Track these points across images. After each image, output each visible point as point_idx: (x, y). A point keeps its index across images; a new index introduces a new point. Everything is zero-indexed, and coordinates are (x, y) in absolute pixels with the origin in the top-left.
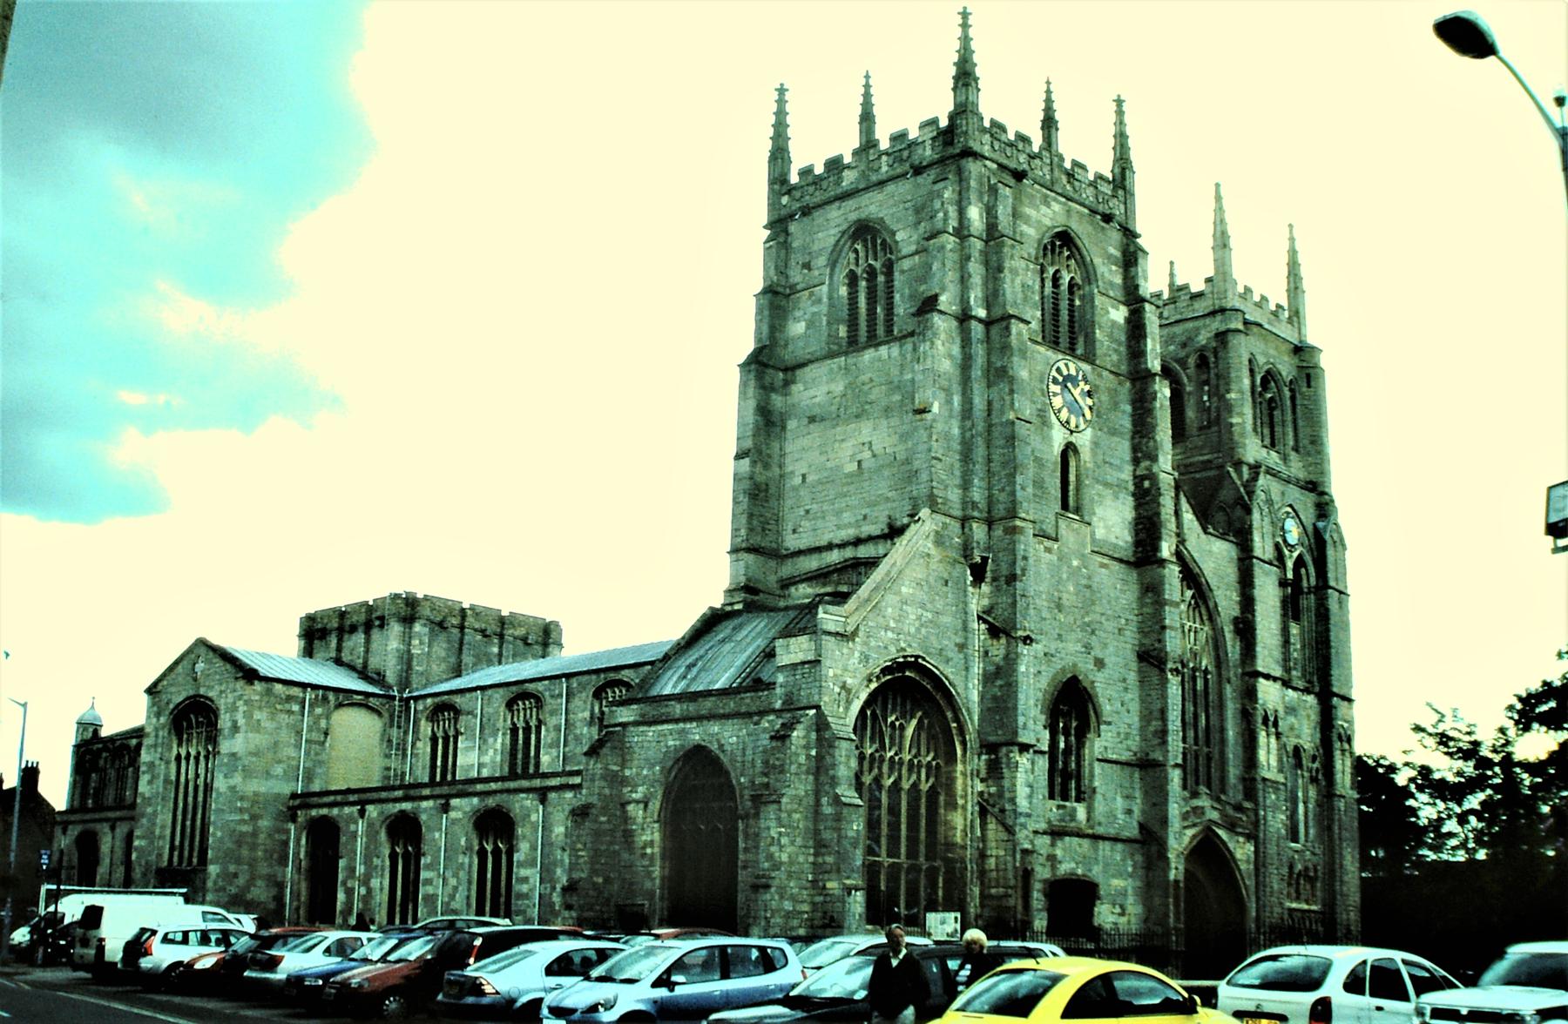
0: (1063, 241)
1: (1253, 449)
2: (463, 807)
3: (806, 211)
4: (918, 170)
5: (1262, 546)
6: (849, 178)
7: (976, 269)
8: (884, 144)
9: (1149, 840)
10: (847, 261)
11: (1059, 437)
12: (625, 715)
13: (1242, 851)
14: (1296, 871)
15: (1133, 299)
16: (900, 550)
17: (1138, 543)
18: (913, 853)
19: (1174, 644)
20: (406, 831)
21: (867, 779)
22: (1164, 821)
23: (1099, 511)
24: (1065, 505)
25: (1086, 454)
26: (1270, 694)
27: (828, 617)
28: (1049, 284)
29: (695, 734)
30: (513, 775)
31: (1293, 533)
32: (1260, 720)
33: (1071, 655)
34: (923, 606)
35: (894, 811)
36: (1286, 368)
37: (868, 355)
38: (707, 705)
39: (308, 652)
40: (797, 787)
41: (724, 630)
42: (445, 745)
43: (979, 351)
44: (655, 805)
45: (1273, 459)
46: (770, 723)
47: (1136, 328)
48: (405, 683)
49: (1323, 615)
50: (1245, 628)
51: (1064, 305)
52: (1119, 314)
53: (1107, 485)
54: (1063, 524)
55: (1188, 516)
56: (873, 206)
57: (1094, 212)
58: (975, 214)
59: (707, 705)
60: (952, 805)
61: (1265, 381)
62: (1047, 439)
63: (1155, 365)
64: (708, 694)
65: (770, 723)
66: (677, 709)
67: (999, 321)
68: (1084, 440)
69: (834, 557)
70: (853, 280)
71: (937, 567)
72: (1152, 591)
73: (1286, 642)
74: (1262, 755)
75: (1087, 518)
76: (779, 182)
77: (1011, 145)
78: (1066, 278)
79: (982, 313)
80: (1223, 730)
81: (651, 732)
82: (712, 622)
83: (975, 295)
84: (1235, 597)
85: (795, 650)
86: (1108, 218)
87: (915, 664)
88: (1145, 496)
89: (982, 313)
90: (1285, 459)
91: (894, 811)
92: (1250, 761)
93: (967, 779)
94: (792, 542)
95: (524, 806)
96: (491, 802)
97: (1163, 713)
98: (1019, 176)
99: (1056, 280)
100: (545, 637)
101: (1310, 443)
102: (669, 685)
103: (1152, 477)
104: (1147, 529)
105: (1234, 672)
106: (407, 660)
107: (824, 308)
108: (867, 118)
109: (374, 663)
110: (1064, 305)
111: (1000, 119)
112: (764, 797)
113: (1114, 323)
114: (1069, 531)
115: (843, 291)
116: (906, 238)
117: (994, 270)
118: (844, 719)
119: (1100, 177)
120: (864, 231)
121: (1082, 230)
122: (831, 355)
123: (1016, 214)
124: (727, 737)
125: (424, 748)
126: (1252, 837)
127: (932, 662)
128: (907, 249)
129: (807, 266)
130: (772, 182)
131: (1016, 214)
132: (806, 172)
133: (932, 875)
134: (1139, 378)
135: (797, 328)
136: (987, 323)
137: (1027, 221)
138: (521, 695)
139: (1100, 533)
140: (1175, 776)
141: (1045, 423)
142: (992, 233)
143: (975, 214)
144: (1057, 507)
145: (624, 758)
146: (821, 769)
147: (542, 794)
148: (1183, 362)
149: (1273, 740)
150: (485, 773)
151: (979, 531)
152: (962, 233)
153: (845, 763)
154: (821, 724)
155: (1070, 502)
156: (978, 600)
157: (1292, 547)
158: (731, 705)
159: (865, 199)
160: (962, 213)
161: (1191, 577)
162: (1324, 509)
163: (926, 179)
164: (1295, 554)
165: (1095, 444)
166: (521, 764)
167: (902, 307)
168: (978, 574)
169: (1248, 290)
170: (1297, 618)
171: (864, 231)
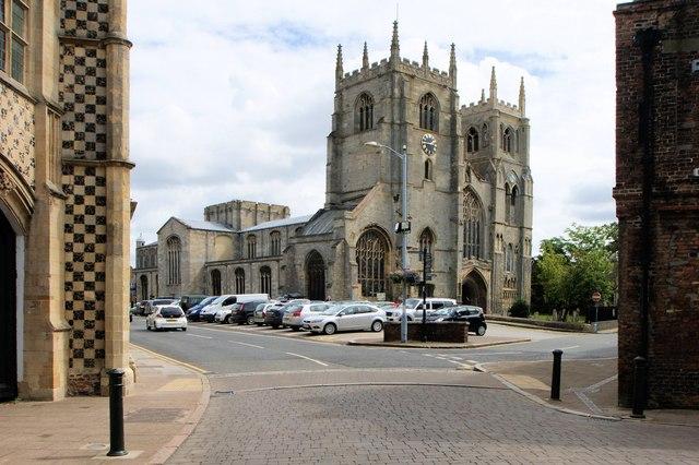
0: (429, 95)
1: (500, 153)
2: (256, 266)
3: (347, 88)
4: (380, 76)
5: (500, 184)
6: (360, 78)
7: (396, 111)
8: (370, 67)
9: (452, 272)
10: (360, 105)
11: (425, 157)
12: (294, 241)
13: (486, 276)
15: (453, 112)
16: (370, 195)
17: (451, 187)
18: (376, 277)
19: (461, 217)
20: (240, 272)
21: (361, 258)
22: (456, 267)
23: (438, 178)
24: (426, 177)
25: (434, 162)
26: (499, 229)
27: (347, 214)
28: (423, 111)
29: (313, 246)
30: (273, 255)
31: (513, 179)
33: (428, 221)
35: (370, 266)
36: (515, 126)
37: (366, 134)
38: (316, 238)
39: (208, 219)
40: (338, 262)
41: (324, 215)
42: (252, 246)
43: (397, 134)
44: (303, 265)
45: (507, 156)
46: (332, 243)
47: (453, 122)
48: (239, 228)
49: (523, 204)
50: (492, 210)
51: (429, 115)
52: (448, 117)
55: (473, 177)
56: (366, 87)
58: (396, 91)
59: (316, 238)
60: (388, 264)
61: (507, 132)
63: (459, 132)
64: (315, 235)
65: (332, 243)
66: (308, 239)
67: (403, 124)
68: (433, 157)
69: (356, 194)
70: (362, 110)
71: (382, 199)
72: (455, 201)
73: (508, 212)
74: (496, 246)
76: (339, 77)
77: (410, 66)
79: (398, 122)
80: (483, 240)
81: (301, 246)
82: (321, 212)
83: (396, 116)
84: (489, 199)
85: (339, 223)
86: (445, 87)
87: (376, 226)
88: (454, 172)
89: (398, 122)
90: (513, 156)
91: (370, 266)
92: (492, 248)
93: (392, 257)
94: (344, 190)
95: (274, 267)
96: (264, 264)
97: (457, 237)
98: (413, 77)
99: (426, 109)
100: (284, 212)
101: (522, 151)
102: (307, 233)
103: (455, 167)
104: (454, 183)
105: (487, 222)
106: (239, 221)
107: (353, 118)
108: (365, 58)
109: (229, 222)
110: (429, 115)
112: (331, 263)
113: (446, 121)
114: (428, 186)
115: (359, 114)
116: (376, 98)
117: (402, 107)
118: (353, 243)
119: (444, 73)
120: (365, 96)
121: (435, 91)
122: (355, 134)
123: (411, 89)
124: (322, 248)
125: (246, 247)
126: (491, 270)
127: (380, 225)
128: (377, 101)
129: (348, 106)
130: (337, 77)
131: (411, 89)
132: (347, 75)
133: (382, 283)
134: (453, 138)
135: (345, 125)
136: (400, 125)
138: (274, 231)
139: (438, 185)
140: (460, 255)
142: (402, 96)
143: (396, 91)
144: (423, 177)
145: (294, 252)
146: (345, 255)
147: (278, 261)
148: (478, 126)
150: (265, 255)
151: (396, 187)
152: (392, 97)
153: (352, 255)
154: (345, 244)
156: (396, 206)
158: (321, 238)
159: (365, 85)
160: (392, 90)
161: (474, 195)
162: (526, 170)
163: (381, 79)
165: (437, 158)
166: (275, 253)
167: (375, 120)
168: (396, 199)
169: (503, 102)
170: (513, 204)
171: (365, 96)
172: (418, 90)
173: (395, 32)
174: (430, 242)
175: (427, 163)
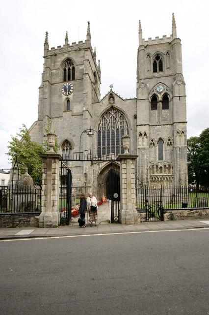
0: (69, 60)
11: (64, 97)
14: (159, 167)
23: (74, 108)
32: (138, 136)
33: (66, 136)
34: (34, 136)
36: (163, 50)
51: (71, 72)
53: (77, 102)
54: (64, 114)
57: (75, 50)
62: (62, 99)
68: (71, 97)
75: (71, 110)
78: (71, 67)
99: (69, 69)
110: (71, 72)
111: (59, 45)
121: (73, 56)
137: (58, 62)
139: (75, 111)
141: (60, 96)
149: (145, 139)
155: (68, 108)
157: (160, 93)
164: (162, 94)
165: (74, 95)
172: (61, 59)
173: (47, 37)
174: (71, 149)
175: (68, 101)
